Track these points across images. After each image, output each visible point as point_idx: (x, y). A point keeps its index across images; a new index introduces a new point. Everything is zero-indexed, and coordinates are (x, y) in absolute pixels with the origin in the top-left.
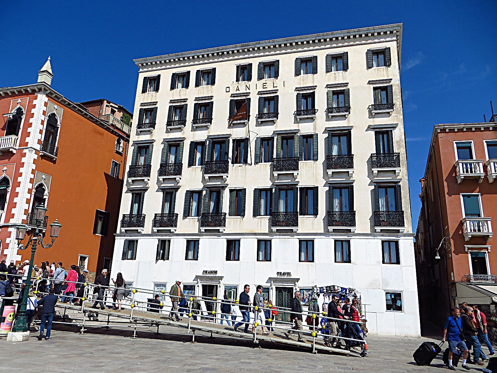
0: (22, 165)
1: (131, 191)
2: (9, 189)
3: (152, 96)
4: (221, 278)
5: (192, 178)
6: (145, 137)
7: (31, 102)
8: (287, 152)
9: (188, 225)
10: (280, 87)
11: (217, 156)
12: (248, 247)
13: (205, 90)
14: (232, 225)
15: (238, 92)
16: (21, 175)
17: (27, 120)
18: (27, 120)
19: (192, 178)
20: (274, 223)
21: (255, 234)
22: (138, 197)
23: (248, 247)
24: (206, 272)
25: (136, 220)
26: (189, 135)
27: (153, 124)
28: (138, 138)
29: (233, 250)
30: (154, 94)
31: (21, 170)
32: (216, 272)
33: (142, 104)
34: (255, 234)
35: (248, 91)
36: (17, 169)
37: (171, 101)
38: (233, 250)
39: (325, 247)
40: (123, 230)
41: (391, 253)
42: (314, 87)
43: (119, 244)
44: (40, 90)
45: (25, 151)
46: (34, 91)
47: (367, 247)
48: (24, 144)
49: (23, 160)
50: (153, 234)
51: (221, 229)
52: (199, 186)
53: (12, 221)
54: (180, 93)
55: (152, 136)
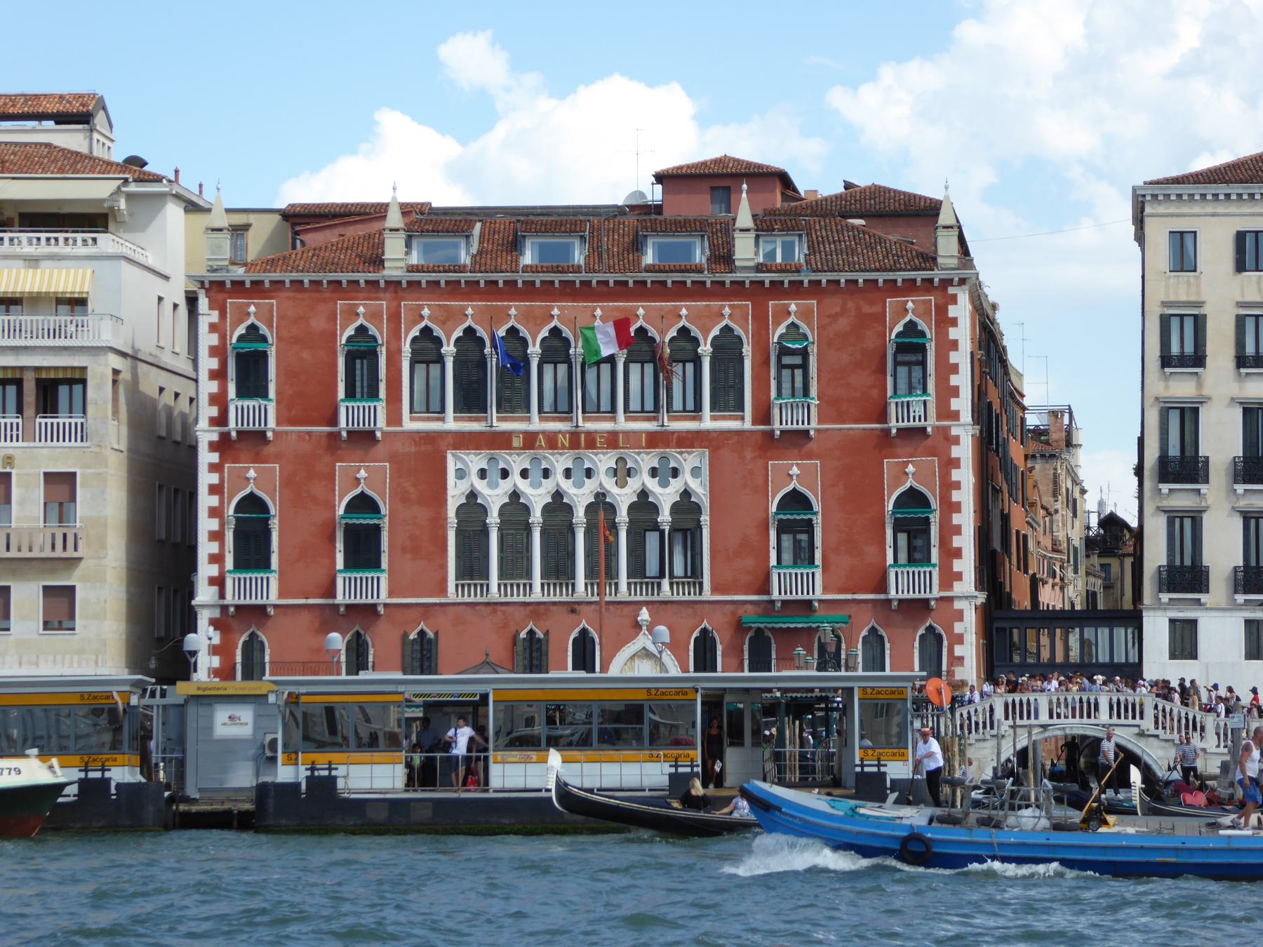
0: (956, 463)
1: (1165, 512)
7: (942, 310)
16: (957, 485)
27: (1198, 359)
28: (1167, 387)
30: (1192, 280)
31: (956, 475)
33: (1165, 304)
36: (945, 475)
37: (1241, 305)
40: (1165, 597)
45: (954, 431)
49: (955, 452)
50: (1235, 607)
53: (959, 588)
54: (1259, 283)
55: (1200, 385)
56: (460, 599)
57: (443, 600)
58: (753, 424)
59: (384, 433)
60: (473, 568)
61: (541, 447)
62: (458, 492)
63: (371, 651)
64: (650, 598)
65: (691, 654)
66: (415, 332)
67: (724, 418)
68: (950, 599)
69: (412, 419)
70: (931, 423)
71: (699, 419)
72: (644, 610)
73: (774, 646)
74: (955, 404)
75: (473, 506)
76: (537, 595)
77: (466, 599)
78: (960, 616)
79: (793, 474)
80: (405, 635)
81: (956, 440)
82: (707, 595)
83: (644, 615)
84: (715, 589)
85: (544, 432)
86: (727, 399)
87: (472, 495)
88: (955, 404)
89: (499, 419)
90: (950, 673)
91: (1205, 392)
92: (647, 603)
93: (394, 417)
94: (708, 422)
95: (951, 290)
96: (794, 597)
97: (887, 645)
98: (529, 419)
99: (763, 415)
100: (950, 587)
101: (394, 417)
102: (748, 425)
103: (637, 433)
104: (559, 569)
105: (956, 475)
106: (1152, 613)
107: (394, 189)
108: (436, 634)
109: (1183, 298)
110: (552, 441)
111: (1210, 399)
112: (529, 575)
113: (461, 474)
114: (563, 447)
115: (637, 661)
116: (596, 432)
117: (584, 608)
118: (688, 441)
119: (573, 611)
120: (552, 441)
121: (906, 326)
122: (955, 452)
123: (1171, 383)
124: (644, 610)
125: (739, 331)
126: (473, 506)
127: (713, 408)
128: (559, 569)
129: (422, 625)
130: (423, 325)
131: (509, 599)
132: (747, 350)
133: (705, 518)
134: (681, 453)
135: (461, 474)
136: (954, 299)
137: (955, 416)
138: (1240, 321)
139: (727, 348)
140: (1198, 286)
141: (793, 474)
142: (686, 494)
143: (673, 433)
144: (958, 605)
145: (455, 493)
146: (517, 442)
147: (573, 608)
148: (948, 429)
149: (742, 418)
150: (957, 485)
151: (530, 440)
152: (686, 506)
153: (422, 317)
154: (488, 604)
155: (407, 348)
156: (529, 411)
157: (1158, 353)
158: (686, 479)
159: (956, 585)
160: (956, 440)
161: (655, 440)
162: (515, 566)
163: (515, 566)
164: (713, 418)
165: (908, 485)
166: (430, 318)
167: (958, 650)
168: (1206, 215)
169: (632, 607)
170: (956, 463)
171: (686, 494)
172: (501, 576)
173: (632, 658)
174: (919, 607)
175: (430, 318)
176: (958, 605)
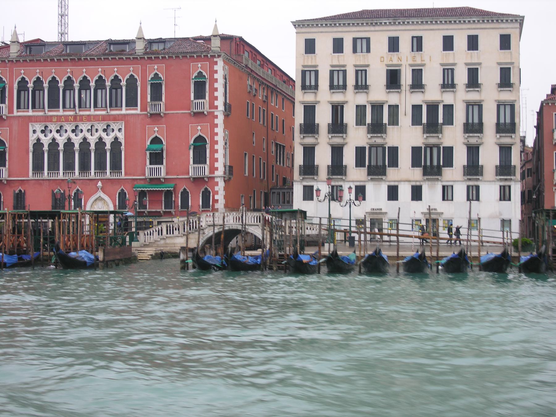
2: (208, 146)
3: (312, 58)
4: (386, 213)
5: (357, 137)
6: (309, 98)
7: (211, 67)
8: (432, 119)
9: (356, 175)
10: (427, 61)
11: (378, 120)
12: (405, 191)
13: (361, 59)
14: (392, 174)
15: (391, 63)
17: (211, 85)
18: (211, 85)
19: (357, 137)
20: (425, 174)
21: (410, 181)
22: (309, 151)
23: (405, 191)
24: (373, 209)
25: (309, 169)
26: (352, 100)
29: (393, 193)
31: (216, 130)
32: (381, 209)
34: (410, 181)
35: (400, 63)
36: (212, 130)
38: (393, 193)
39: (460, 191)
41: (505, 195)
42: (454, 64)
43: (298, 190)
44: (219, 56)
45: (216, 114)
46: (213, 57)
47: (489, 190)
48: (213, 106)
49: (216, 121)
51: (384, 178)
52: (361, 144)
53: (217, 173)
55: (316, 96)
56: (34, 178)
57: (27, 179)
58: (141, 111)
59: (7, 117)
60: (38, 168)
61: (63, 121)
62: (33, 138)
63: (2, 197)
64: (101, 178)
65: (117, 199)
66: (19, 79)
67: (130, 109)
68: (214, 178)
69: (18, 112)
70: (206, 109)
71: (121, 110)
72: (100, 182)
73: (147, 196)
74: (216, 103)
75: (38, 144)
76: (61, 176)
77: (36, 178)
78: (217, 184)
79: (156, 130)
80: (14, 191)
81: (216, 117)
82: (123, 176)
83: (100, 184)
84: (126, 174)
85: (64, 116)
86: (131, 102)
87: (38, 140)
88: (216, 103)
89: (48, 111)
90: (213, 205)
91: (318, 99)
92: (101, 180)
93: (11, 111)
94: (124, 111)
95: (215, 60)
96: (153, 177)
97: (190, 195)
98: (59, 111)
99: (144, 109)
100: (214, 173)
101: (11, 111)
102: (138, 111)
103: (99, 115)
104: (69, 167)
105: (216, 130)
106: (297, 183)
107: (15, 27)
108: (24, 191)
109: (310, 64)
110: (67, 119)
111: (319, 102)
112: (58, 170)
113: (34, 131)
114: (71, 121)
115: (98, 201)
116: (83, 115)
117: (78, 181)
118: (115, 118)
119: (74, 183)
120: (67, 119)
121: (198, 73)
122: (216, 121)
123: (306, 95)
124: (100, 182)
125: (136, 77)
126: (38, 144)
127: (127, 106)
128: (69, 167)
129: (20, 188)
130: (21, 76)
131: (52, 178)
132: (139, 83)
133: (123, 147)
134: (114, 123)
135: (34, 131)
136: (216, 63)
137: (216, 107)
138: (332, 72)
139: (132, 81)
140: (315, 59)
141: (156, 130)
142: (116, 138)
143: (112, 115)
144: (216, 180)
145: (32, 138)
146: (54, 120)
147: (74, 181)
148: (214, 112)
149: (137, 109)
150: (217, 134)
151: (59, 118)
152: (116, 143)
153: (21, 74)
154: (43, 180)
155: (16, 86)
156: (59, 108)
157: (300, 84)
158: (116, 131)
159: (216, 172)
160: (216, 117)
161: (104, 118)
162: (54, 166)
163: (54, 166)
164: (126, 110)
165: (198, 134)
166: (24, 74)
167: (216, 197)
168: (319, 32)
169: (95, 181)
170: (216, 126)
171: (116, 138)
172: (48, 170)
173: (96, 200)
174: (198, 181)
175: (24, 74)
176: (216, 180)
